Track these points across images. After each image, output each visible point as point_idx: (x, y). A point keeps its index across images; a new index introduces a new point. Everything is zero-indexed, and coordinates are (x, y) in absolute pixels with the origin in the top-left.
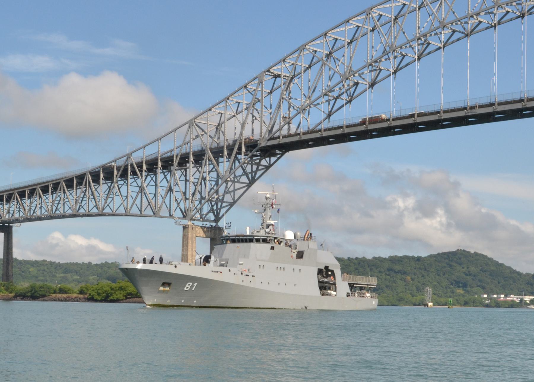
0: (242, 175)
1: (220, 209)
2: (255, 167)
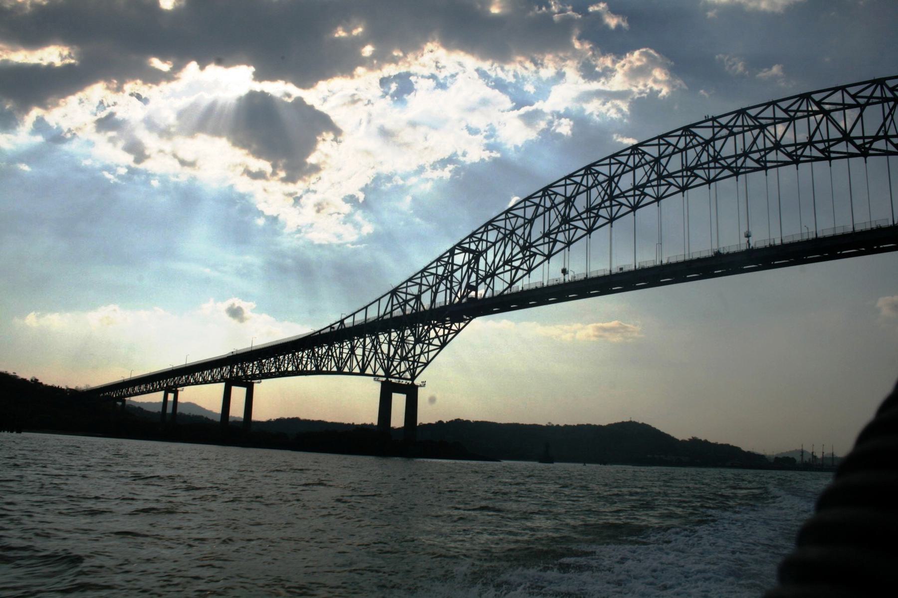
0: (435, 338)
2: (446, 331)
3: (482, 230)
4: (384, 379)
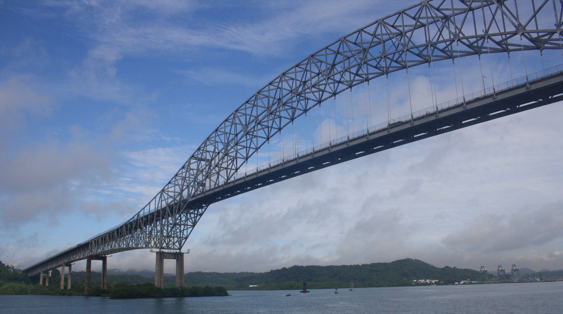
4: (158, 250)
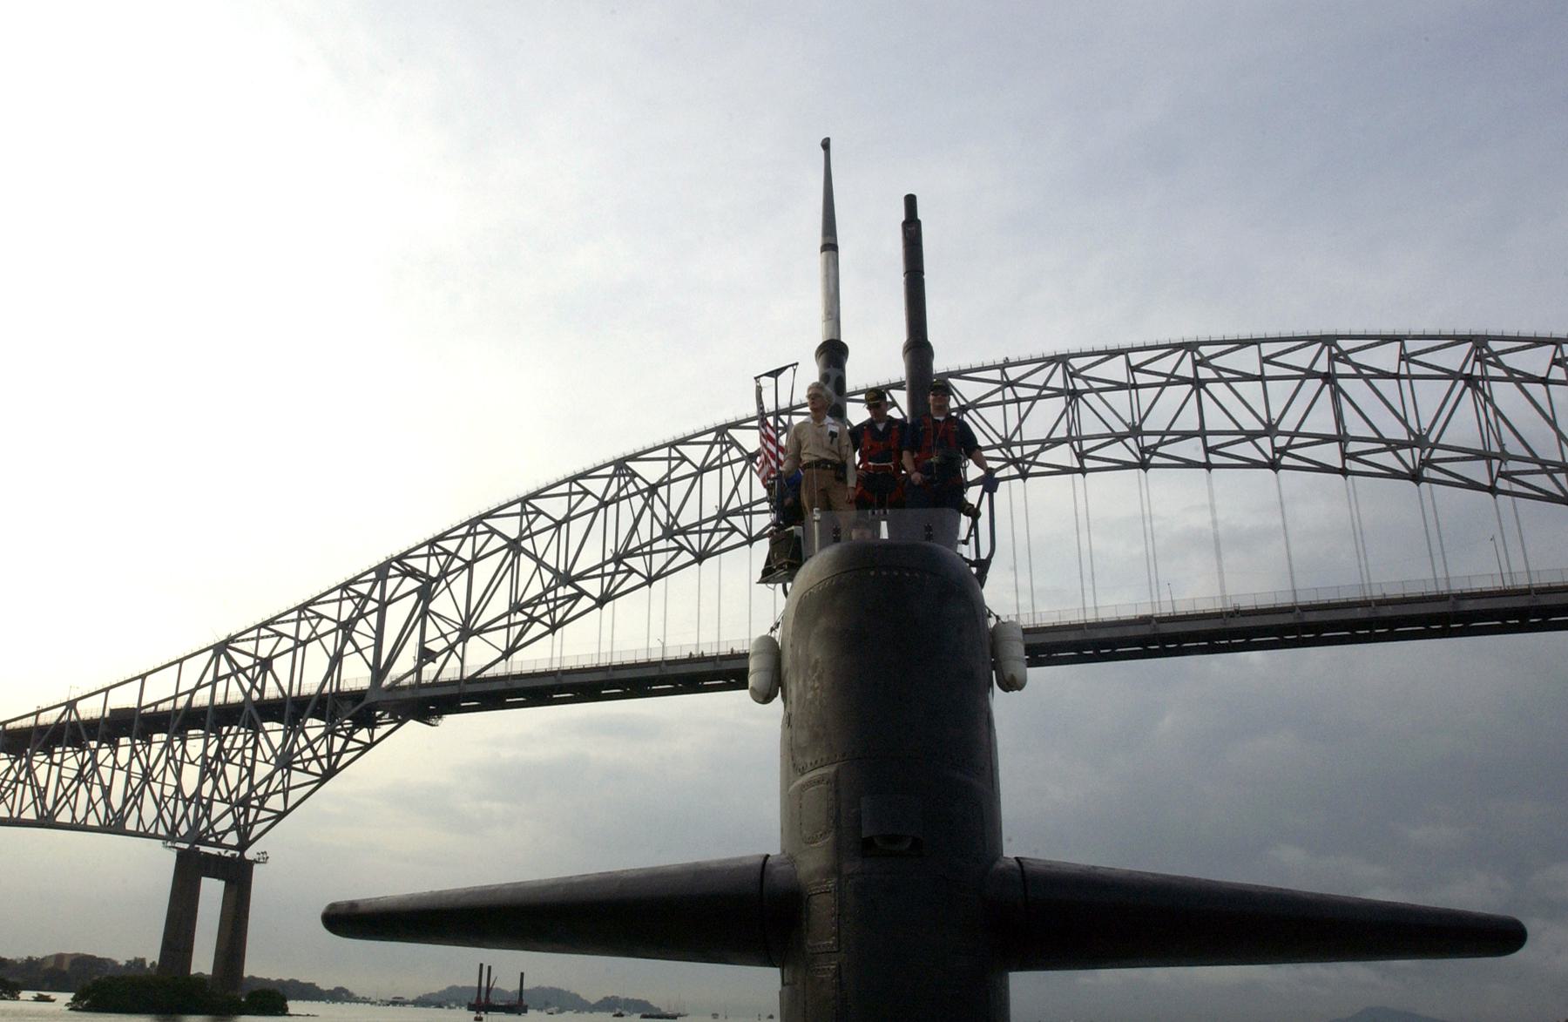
1: (252, 825)
3: (463, 531)
